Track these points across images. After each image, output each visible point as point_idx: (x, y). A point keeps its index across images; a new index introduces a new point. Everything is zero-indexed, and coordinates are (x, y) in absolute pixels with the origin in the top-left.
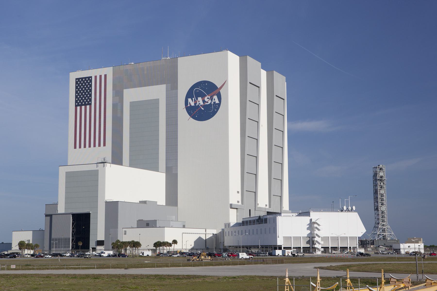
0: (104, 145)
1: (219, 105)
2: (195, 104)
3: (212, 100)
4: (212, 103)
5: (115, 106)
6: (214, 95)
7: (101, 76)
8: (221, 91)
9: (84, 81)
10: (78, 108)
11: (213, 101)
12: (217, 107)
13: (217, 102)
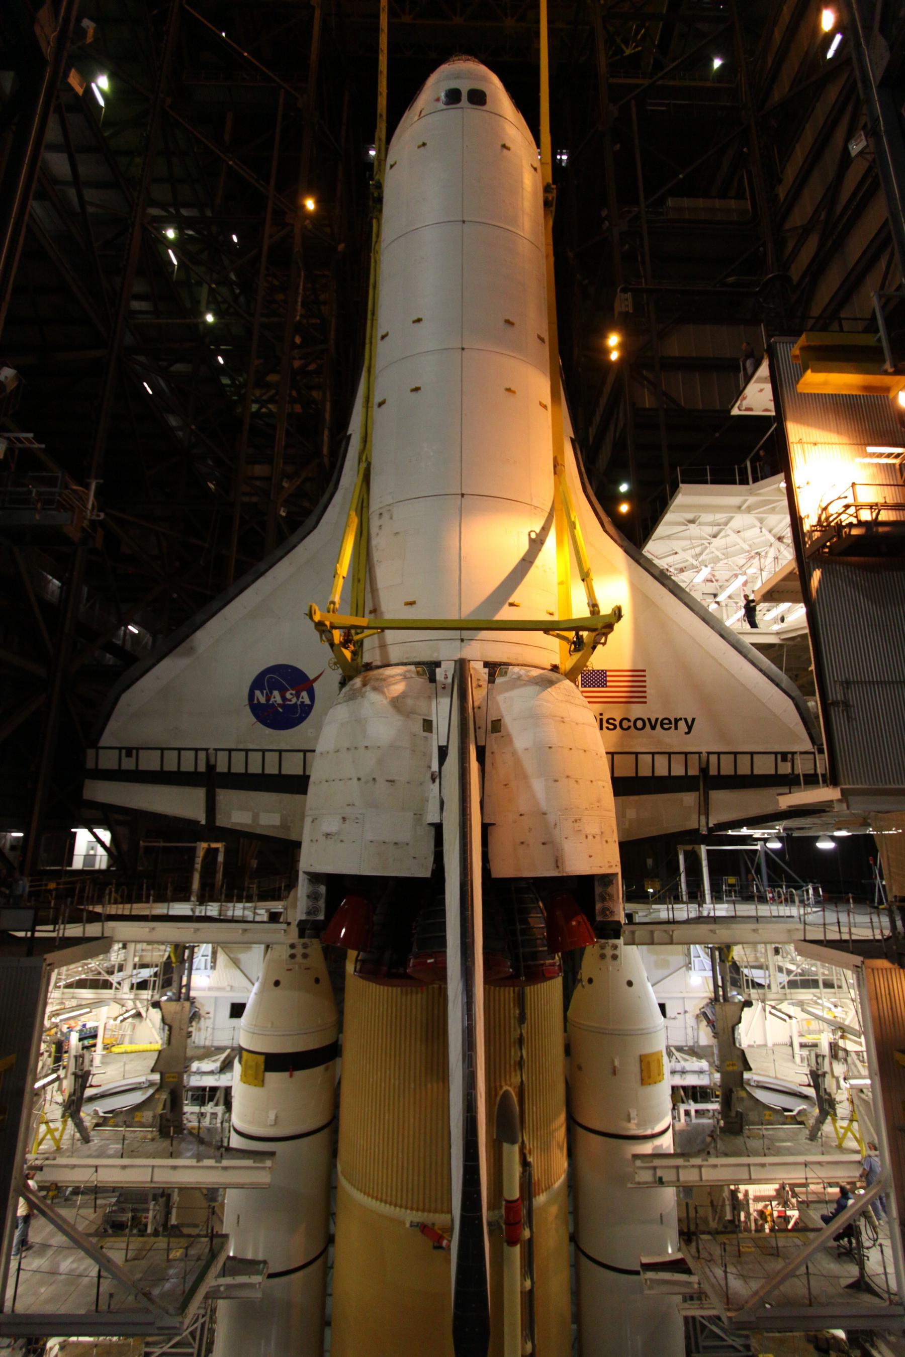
1: (310, 707)
3: (298, 698)
4: (299, 703)
6: (302, 690)
8: (315, 685)
11: (301, 700)
12: (306, 710)
13: (307, 701)
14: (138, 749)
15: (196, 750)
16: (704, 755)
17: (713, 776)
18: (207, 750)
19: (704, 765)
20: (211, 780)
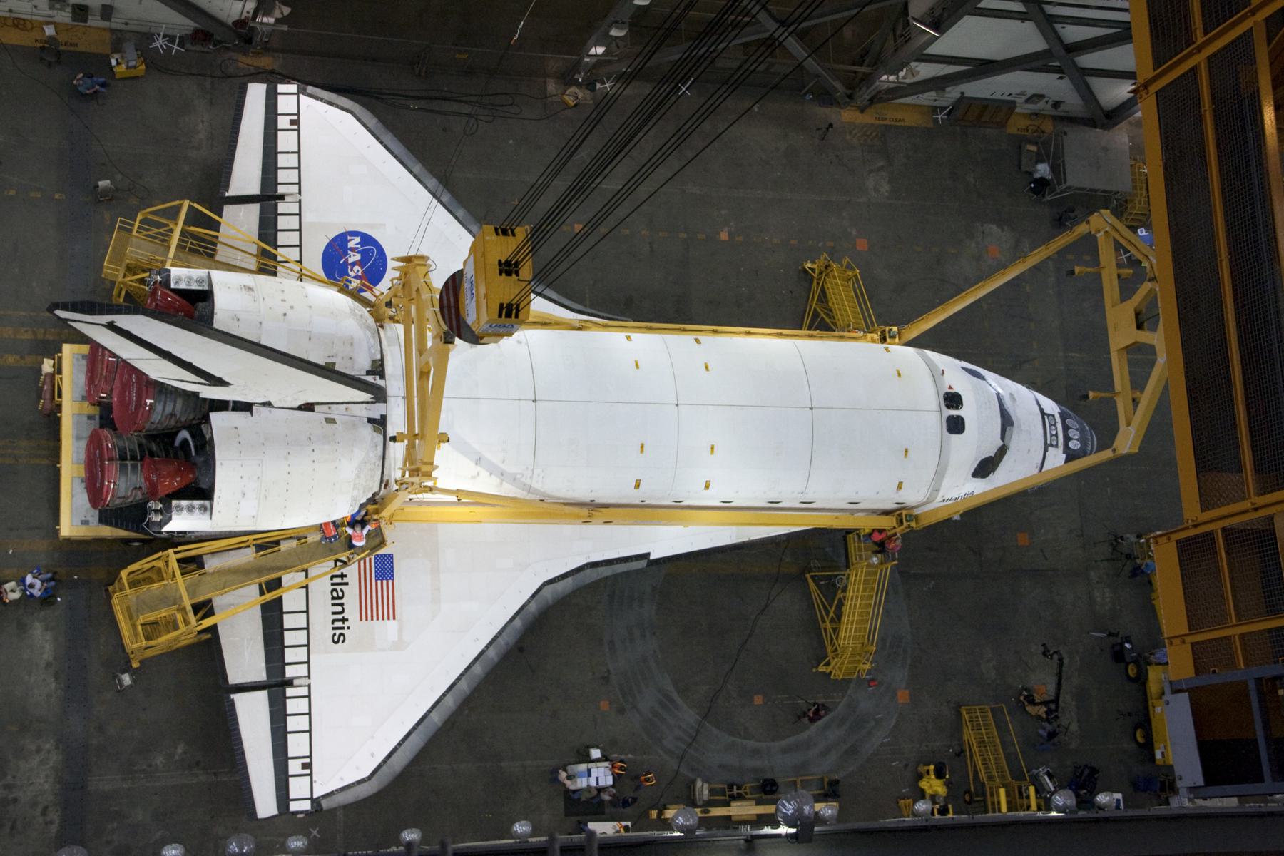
2: (352, 249)
14: (298, 130)
15: (299, 184)
16: (306, 681)
17: (284, 692)
18: (300, 193)
19: (296, 682)
20: (269, 198)
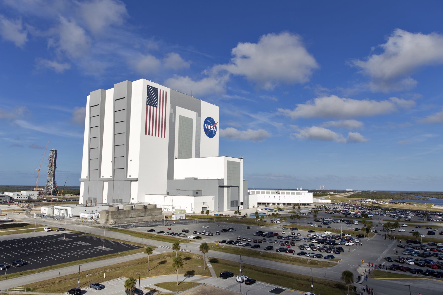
0: (165, 137)
5: (171, 114)
7: (163, 91)
9: (153, 90)
10: (149, 106)
